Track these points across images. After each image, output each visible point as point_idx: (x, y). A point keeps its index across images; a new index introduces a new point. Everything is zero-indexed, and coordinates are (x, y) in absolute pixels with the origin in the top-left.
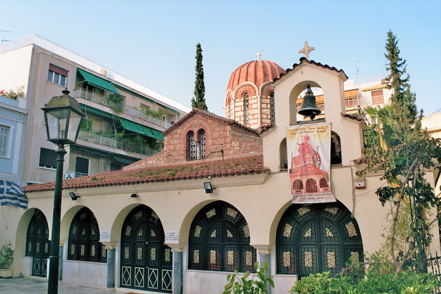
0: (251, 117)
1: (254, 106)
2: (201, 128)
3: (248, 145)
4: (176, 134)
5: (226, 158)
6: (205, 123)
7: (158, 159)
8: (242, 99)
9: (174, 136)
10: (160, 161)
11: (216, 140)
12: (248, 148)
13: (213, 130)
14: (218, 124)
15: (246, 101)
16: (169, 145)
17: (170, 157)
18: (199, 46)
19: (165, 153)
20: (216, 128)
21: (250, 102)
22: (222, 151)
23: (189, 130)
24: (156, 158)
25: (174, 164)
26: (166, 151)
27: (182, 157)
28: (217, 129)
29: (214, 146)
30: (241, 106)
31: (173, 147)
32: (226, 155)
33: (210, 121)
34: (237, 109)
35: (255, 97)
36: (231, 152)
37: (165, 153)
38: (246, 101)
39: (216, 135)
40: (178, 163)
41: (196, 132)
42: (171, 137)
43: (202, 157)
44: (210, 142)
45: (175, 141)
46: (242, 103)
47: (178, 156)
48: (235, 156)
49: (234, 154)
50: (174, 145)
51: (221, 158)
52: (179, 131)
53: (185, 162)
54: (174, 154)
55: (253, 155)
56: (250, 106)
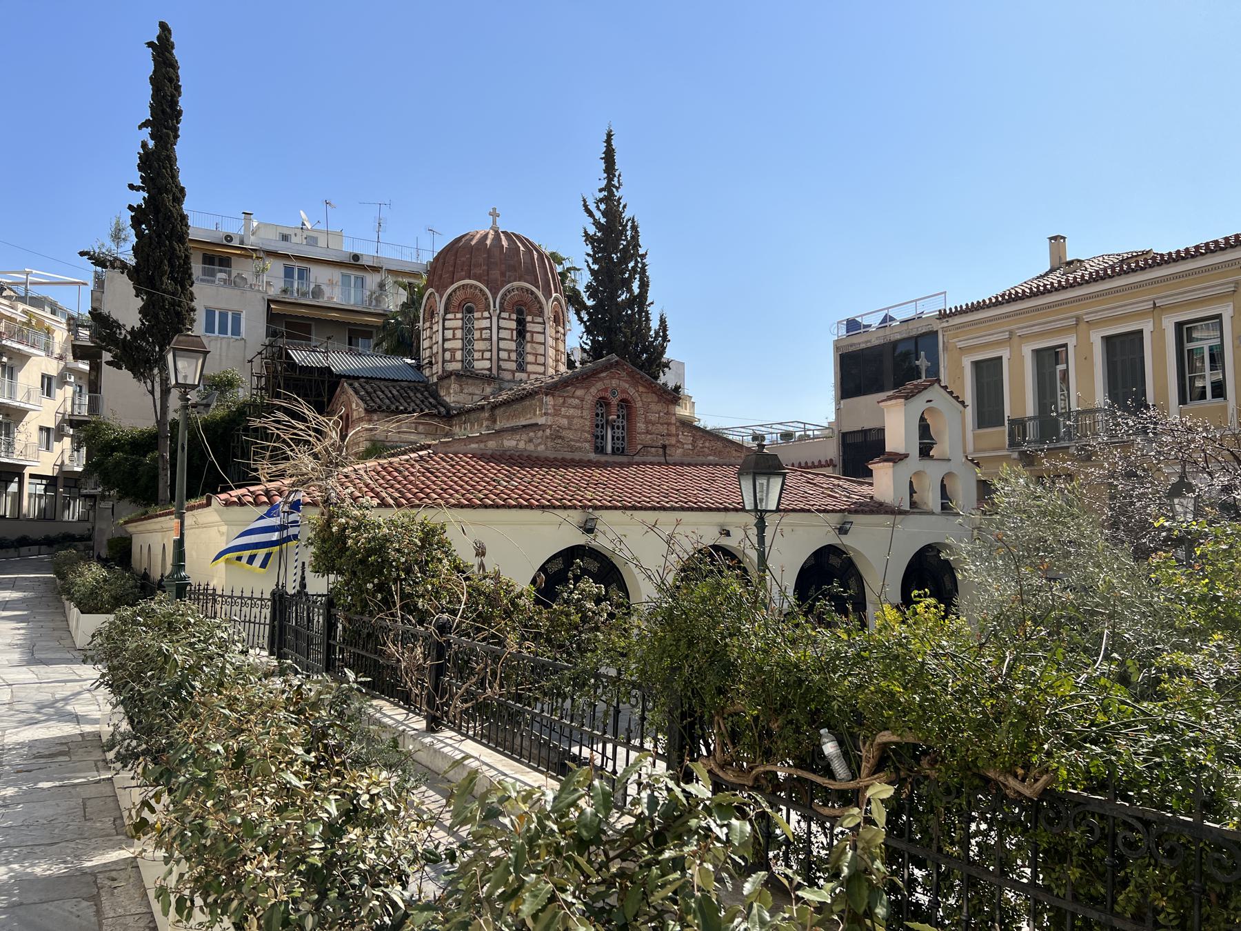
0: (530, 358)
1: (540, 338)
2: (624, 396)
6: (632, 391)
7: (531, 441)
8: (514, 316)
9: (570, 401)
10: (536, 446)
15: (521, 323)
18: (162, 49)
21: (529, 327)
23: (603, 394)
24: (524, 437)
26: (550, 426)
28: (654, 407)
30: (512, 330)
31: (565, 422)
33: (641, 389)
34: (503, 334)
35: (540, 320)
36: (680, 451)
38: (521, 323)
39: (653, 417)
41: (614, 401)
42: (561, 400)
43: (613, 452)
44: (641, 426)
45: (571, 411)
46: (513, 325)
47: (578, 441)
50: (567, 417)
52: (579, 393)
54: (569, 434)
56: (528, 335)
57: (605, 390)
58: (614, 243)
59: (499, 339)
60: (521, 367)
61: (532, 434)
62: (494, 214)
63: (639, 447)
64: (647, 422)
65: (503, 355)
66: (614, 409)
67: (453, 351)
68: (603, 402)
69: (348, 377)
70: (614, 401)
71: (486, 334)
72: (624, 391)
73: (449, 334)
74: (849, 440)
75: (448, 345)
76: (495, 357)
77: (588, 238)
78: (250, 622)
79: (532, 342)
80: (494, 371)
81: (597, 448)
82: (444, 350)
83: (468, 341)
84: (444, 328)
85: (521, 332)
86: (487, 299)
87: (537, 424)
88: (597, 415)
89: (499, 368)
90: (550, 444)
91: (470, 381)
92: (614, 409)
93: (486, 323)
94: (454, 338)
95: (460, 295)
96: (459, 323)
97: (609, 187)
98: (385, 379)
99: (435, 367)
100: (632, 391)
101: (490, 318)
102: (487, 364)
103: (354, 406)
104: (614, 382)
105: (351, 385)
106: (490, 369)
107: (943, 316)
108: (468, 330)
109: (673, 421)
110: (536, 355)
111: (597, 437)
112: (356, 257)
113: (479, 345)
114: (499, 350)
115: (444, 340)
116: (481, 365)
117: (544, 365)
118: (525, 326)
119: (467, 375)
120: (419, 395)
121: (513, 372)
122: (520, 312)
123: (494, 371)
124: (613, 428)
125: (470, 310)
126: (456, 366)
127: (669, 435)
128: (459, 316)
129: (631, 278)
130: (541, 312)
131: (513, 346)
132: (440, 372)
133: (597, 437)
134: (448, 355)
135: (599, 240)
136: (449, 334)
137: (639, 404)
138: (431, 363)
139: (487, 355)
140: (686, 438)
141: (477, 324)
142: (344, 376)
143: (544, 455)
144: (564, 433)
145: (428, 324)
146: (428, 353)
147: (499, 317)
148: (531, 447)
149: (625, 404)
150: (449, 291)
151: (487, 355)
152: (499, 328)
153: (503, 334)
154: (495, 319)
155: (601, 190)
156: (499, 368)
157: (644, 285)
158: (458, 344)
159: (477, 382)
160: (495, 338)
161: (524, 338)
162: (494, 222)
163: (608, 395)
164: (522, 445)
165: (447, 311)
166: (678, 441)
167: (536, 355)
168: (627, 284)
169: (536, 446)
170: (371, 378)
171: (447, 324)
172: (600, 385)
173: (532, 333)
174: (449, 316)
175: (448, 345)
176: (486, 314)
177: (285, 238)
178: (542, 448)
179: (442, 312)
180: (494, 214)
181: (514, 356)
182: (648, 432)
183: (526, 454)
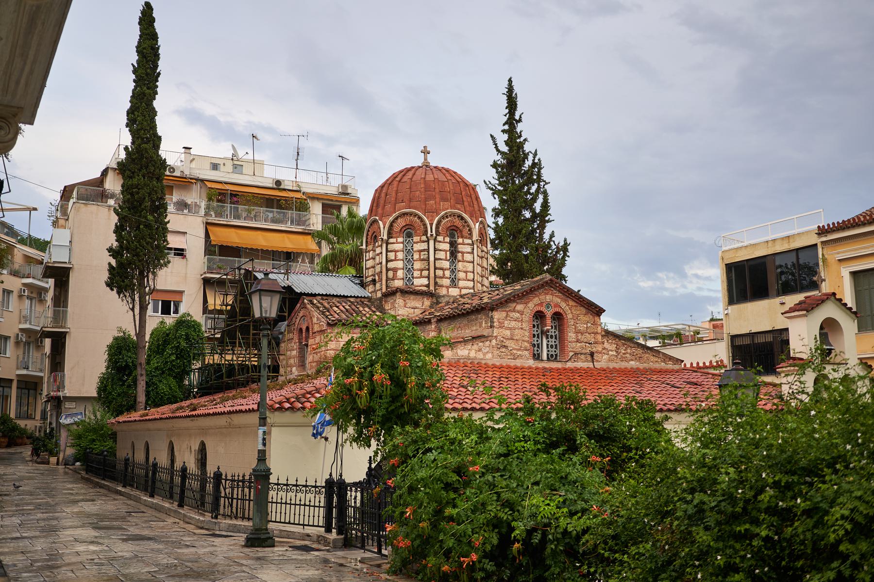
0: (461, 275)
2: (557, 309)
3: (629, 351)
4: (514, 311)
5: (598, 365)
6: (563, 305)
7: (480, 350)
8: (448, 239)
10: (484, 354)
11: (582, 334)
12: (628, 355)
13: (576, 318)
14: (584, 310)
16: (502, 327)
17: (504, 350)
19: (494, 341)
20: (581, 317)
21: (461, 248)
22: (592, 354)
24: (475, 347)
25: (512, 363)
27: (526, 353)
29: (579, 344)
30: (446, 251)
32: (597, 361)
33: (571, 303)
34: (441, 255)
35: (470, 241)
36: (605, 357)
37: (494, 341)
38: (453, 244)
39: (582, 327)
40: (518, 363)
41: (549, 313)
42: (504, 314)
44: (571, 336)
45: (513, 324)
46: (447, 247)
47: (518, 350)
48: (612, 365)
49: (609, 360)
50: (510, 329)
51: (591, 365)
52: (520, 307)
53: (531, 363)
54: (511, 344)
55: (635, 367)
56: (460, 255)
57: (541, 304)
58: (517, 170)
59: (435, 259)
60: (454, 283)
61: (481, 344)
62: (425, 152)
63: (571, 354)
64: (577, 332)
65: (439, 273)
66: (549, 321)
67: (395, 270)
68: (539, 316)
69: (308, 295)
70: (549, 313)
71: (424, 255)
72: (557, 305)
73: (391, 256)
74: (739, 342)
75: (391, 265)
76: (432, 275)
77: (495, 165)
78: (305, 505)
79: (463, 261)
80: (432, 288)
81: (534, 355)
82: (388, 270)
83: (409, 260)
84: (387, 251)
85: (454, 252)
86: (425, 225)
87: (483, 336)
88: (534, 326)
89: (436, 283)
90: (496, 352)
91: (412, 297)
92: (549, 321)
93: (424, 246)
94: (396, 260)
95: (401, 222)
96: (399, 247)
97: (512, 122)
98: (337, 296)
99: (378, 285)
100: (563, 305)
101: (428, 241)
102: (425, 281)
103: (315, 320)
104: (549, 298)
105: (311, 302)
106: (428, 286)
107: (822, 231)
108: (409, 252)
109: (599, 331)
110: (466, 272)
111: (534, 345)
112: (278, 183)
113: (417, 265)
114: (435, 268)
115: (387, 261)
116: (420, 283)
117: (473, 280)
118: (456, 247)
119: (408, 292)
120: (367, 309)
121: (448, 287)
122: (452, 236)
123: (432, 288)
124: (547, 338)
125: (409, 235)
126: (398, 283)
127: (596, 343)
128: (400, 240)
129: (534, 200)
130: (470, 235)
131: (446, 264)
132: (384, 290)
133: (534, 345)
134: (391, 274)
135: (502, 166)
136: (391, 256)
137: (570, 316)
138: (374, 282)
139: (425, 273)
140: (610, 345)
141: (417, 247)
142: (305, 294)
143: (490, 363)
144: (507, 343)
145: (370, 247)
146: (371, 272)
147: (435, 240)
148: (480, 355)
149: (558, 317)
150: (391, 219)
151: (425, 273)
152: (435, 250)
153: (441, 255)
154: (432, 242)
155: (504, 125)
156: (436, 283)
157: (545, 206)
158: (400, 264)
159: (418, 297)
160: (432, 259)
161: (456, 257)
162: (426, 159)
163: (543, 309)
164: (473, 354)
165: (390, 235)
166: (604, 349)
167: (466, 272)
168: (529, 206)
169: (484, 354)
170: (326, 295)
171: (390, 247)
172: (536, 300)
173: (463, 253)
174: (391, 240)
175: (391, 265)
176: (424, 238)
177: (215, 167)
178: (489, 356)
179: (385, 237)
180: (425, 152)
181: (447, 273)
182: (578, 341)
183: (483, 362)
